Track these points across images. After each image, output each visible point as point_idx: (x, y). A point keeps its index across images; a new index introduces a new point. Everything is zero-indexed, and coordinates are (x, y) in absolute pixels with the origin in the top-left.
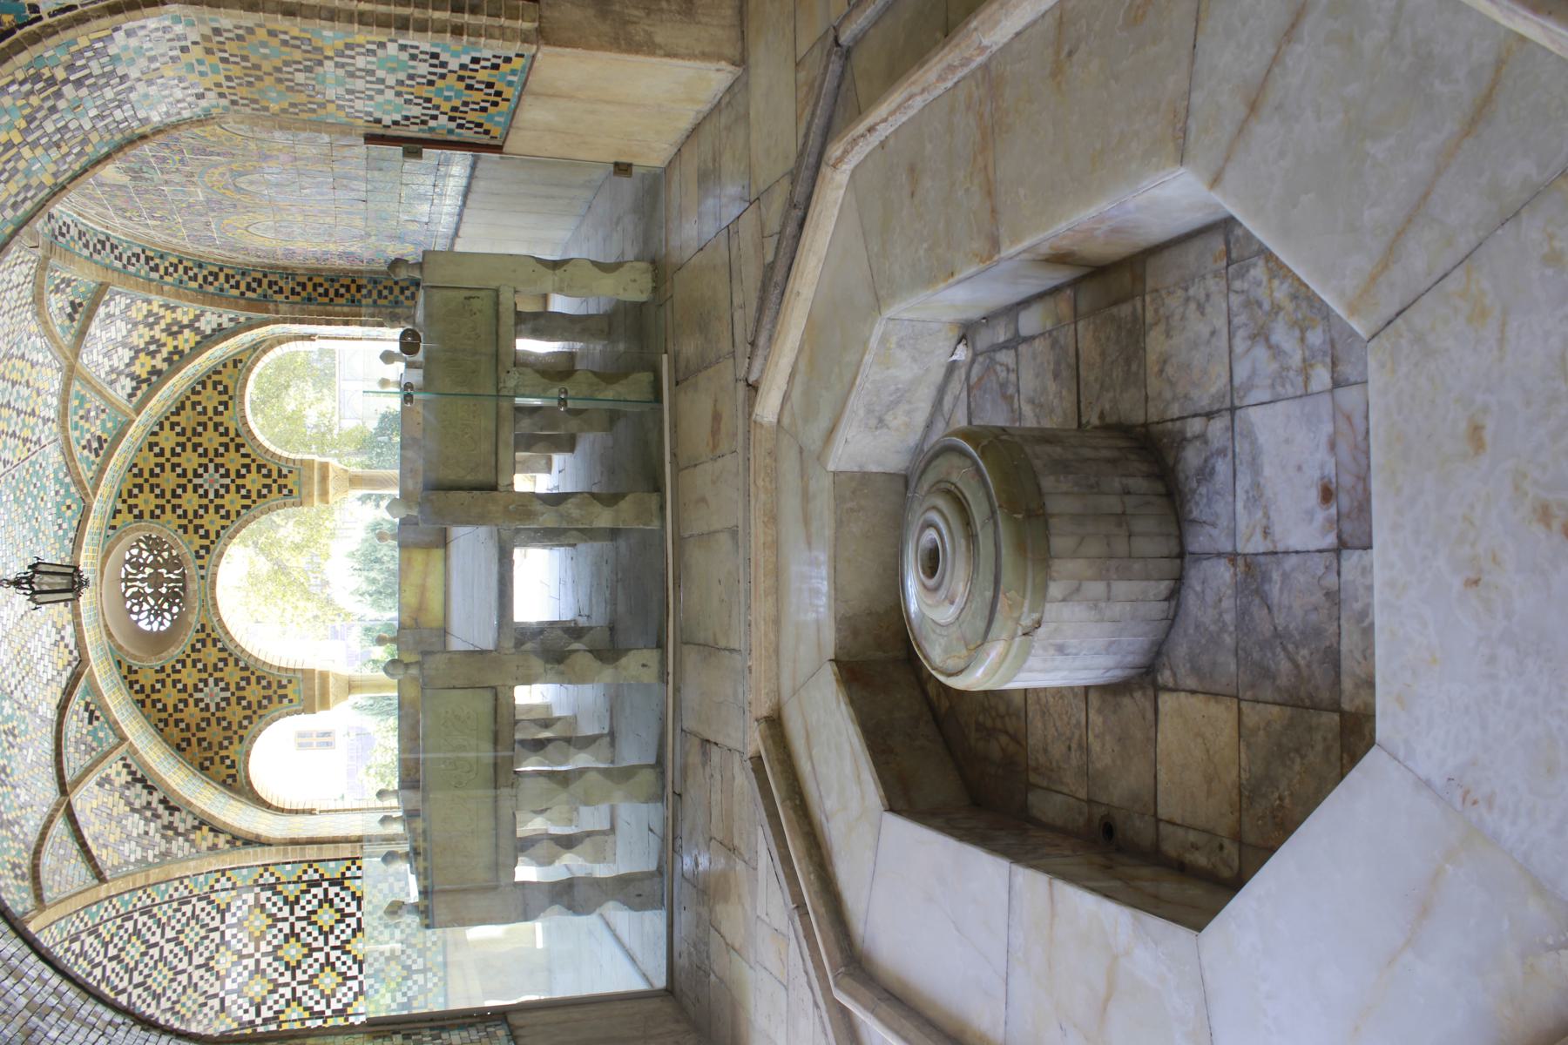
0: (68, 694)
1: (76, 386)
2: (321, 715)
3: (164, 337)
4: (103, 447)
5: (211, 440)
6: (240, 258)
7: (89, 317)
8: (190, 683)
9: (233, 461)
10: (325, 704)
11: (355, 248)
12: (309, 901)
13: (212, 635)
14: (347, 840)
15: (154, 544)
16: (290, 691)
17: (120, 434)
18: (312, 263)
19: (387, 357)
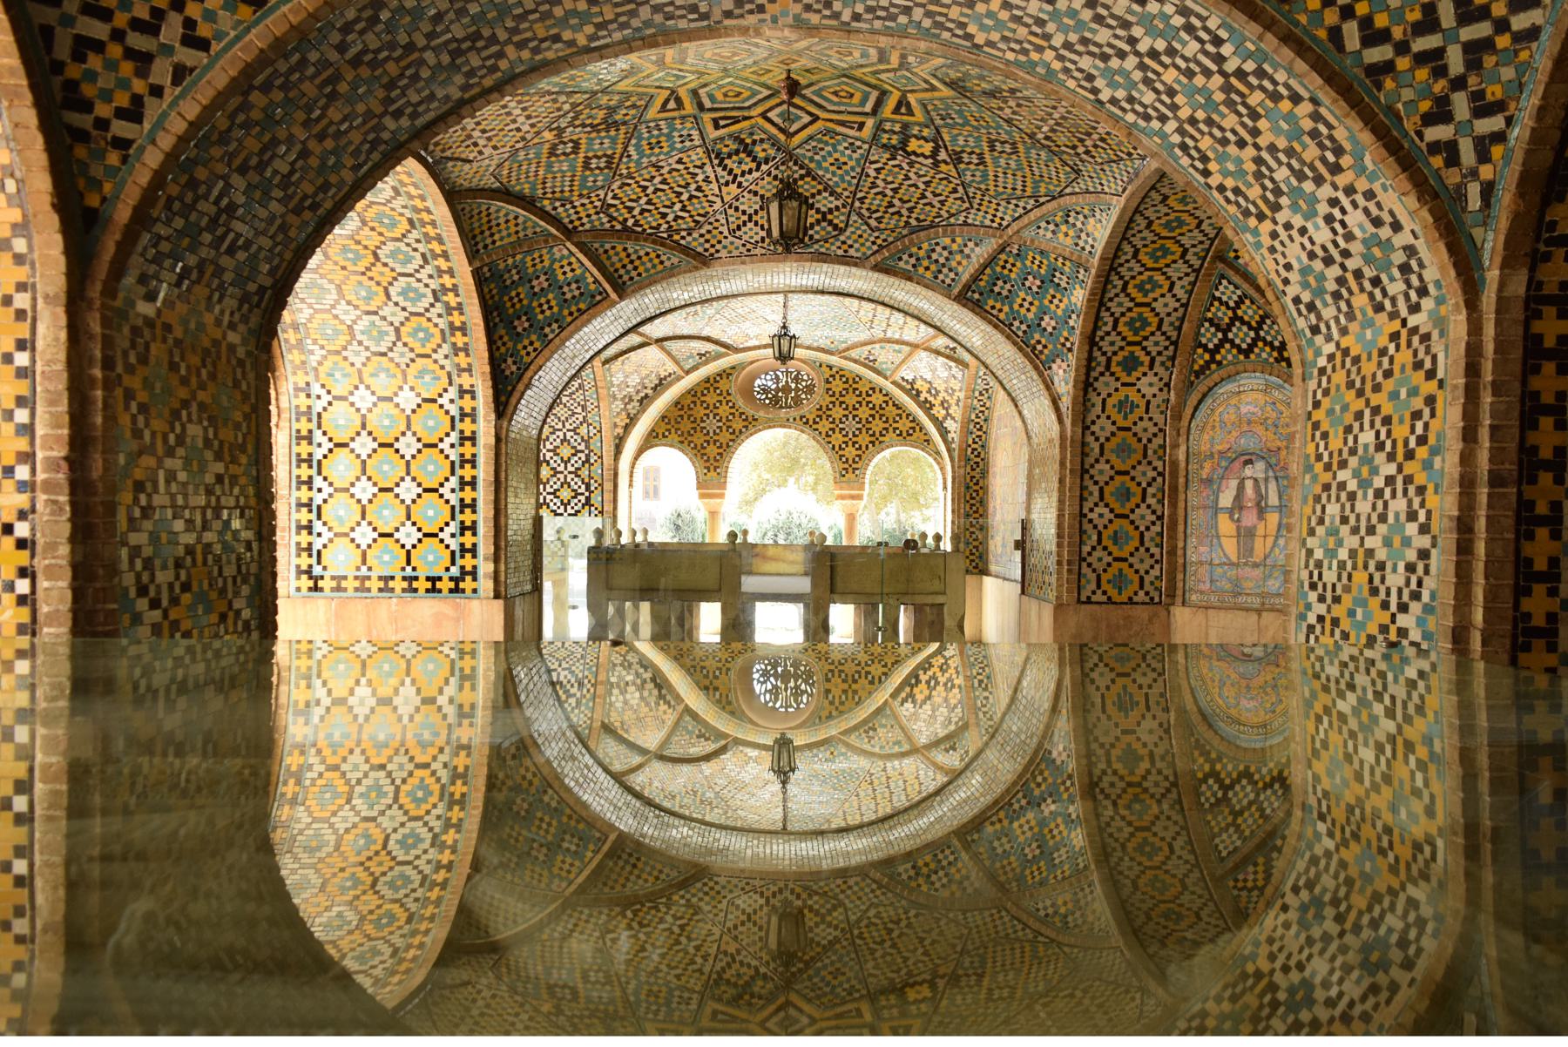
0: (716, 342)
1: (907, 349)
2: (696, 493)
3: (940, 398)
4: (870, 364)
5: (877, 426)
6: (992, 445)
7: (948, 357)
8: (720, 411)
9: (864, 439)
10: (702, 496)
11: (998, 517)
12: (576, 484)
13: (750, 425)
14: (615, 508)
15: (810, 389)
16: (712, 474)
17: (878, 372)
18: (991, 489)
19: (938, 538)
